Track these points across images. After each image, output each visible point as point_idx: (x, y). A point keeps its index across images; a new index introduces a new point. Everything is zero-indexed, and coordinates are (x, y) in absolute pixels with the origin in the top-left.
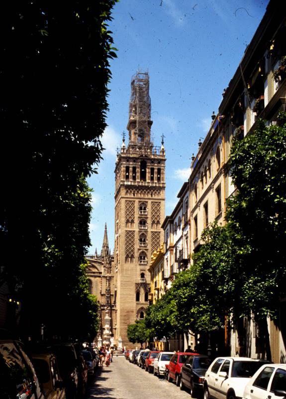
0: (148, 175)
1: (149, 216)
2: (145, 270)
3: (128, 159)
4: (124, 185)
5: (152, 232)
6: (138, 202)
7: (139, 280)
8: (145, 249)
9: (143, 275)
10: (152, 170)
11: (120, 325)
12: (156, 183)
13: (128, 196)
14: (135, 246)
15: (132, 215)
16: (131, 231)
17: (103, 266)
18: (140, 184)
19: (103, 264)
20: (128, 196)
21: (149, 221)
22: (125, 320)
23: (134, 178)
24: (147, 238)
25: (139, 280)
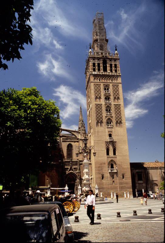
0: (108, 68)
1: (112, 94)
2: (112, 132)
3: (94, 58)
4: (92, 74)
5: (115, 105)
6: (103, 85)
7: (108, 139)
8: (111, 117)
9: (110, 135)
10: (111, 65)
11: (96, 175)
12: (114, 73)
13: (96, 81)
14: (103, 115)
15: (99, 93)
16: (99, 104)
17: (80, 134)
18: (104, 73)
19: (80, 133)
20: (96, 81)
21: (112, 97)
22: (99, 170)
23: (99, 70)
24: (111, 109)
25: (108, 139)
